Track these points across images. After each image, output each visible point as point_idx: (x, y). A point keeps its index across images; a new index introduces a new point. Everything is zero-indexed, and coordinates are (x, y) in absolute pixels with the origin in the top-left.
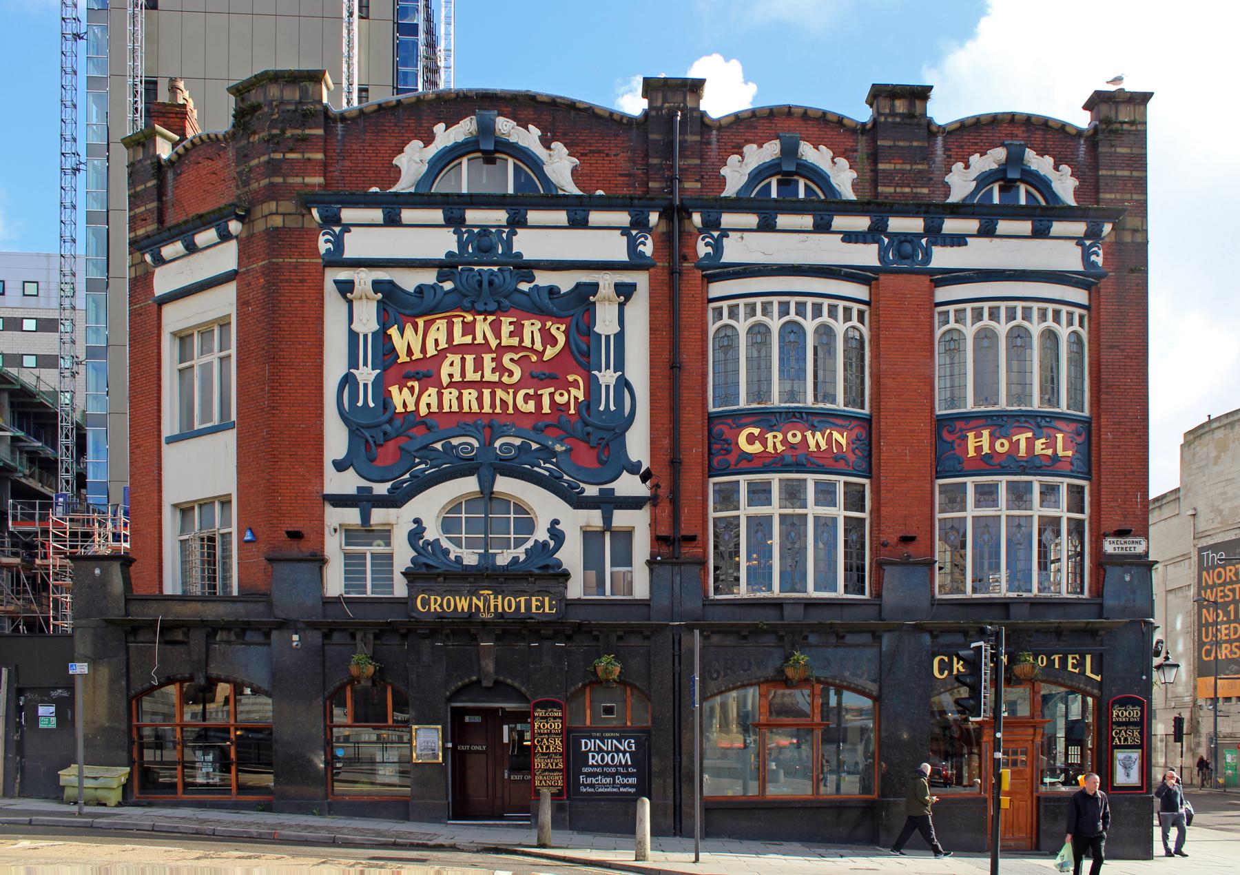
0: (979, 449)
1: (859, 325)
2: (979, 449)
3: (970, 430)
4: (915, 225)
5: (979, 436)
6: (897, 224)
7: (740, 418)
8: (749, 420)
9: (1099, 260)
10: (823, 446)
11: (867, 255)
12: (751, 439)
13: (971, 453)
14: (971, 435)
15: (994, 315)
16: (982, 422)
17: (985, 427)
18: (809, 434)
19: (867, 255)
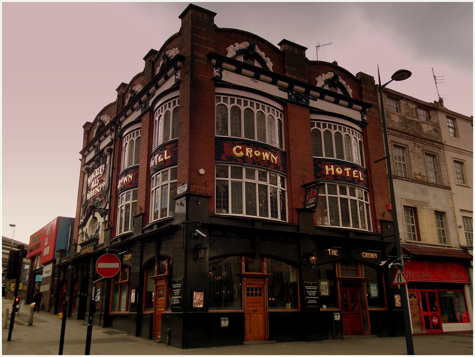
0: (330, 172)
1: (280, 119)
2: (330, 172)
3: (327, 164)
4: (302, 90)
5: (330, 167)
6: (296, 87)
7: (234, 142)
8: (238, 142)
9: (365, 118)
10: (268, 159)
11: (284, 95)
12: (238, 151)
13: (327, 173)
14: (327, 167)
15: (330, 126)
16: (330, 163)
17: (332, 164)
18: (263, 153)
19: (284, 95)
